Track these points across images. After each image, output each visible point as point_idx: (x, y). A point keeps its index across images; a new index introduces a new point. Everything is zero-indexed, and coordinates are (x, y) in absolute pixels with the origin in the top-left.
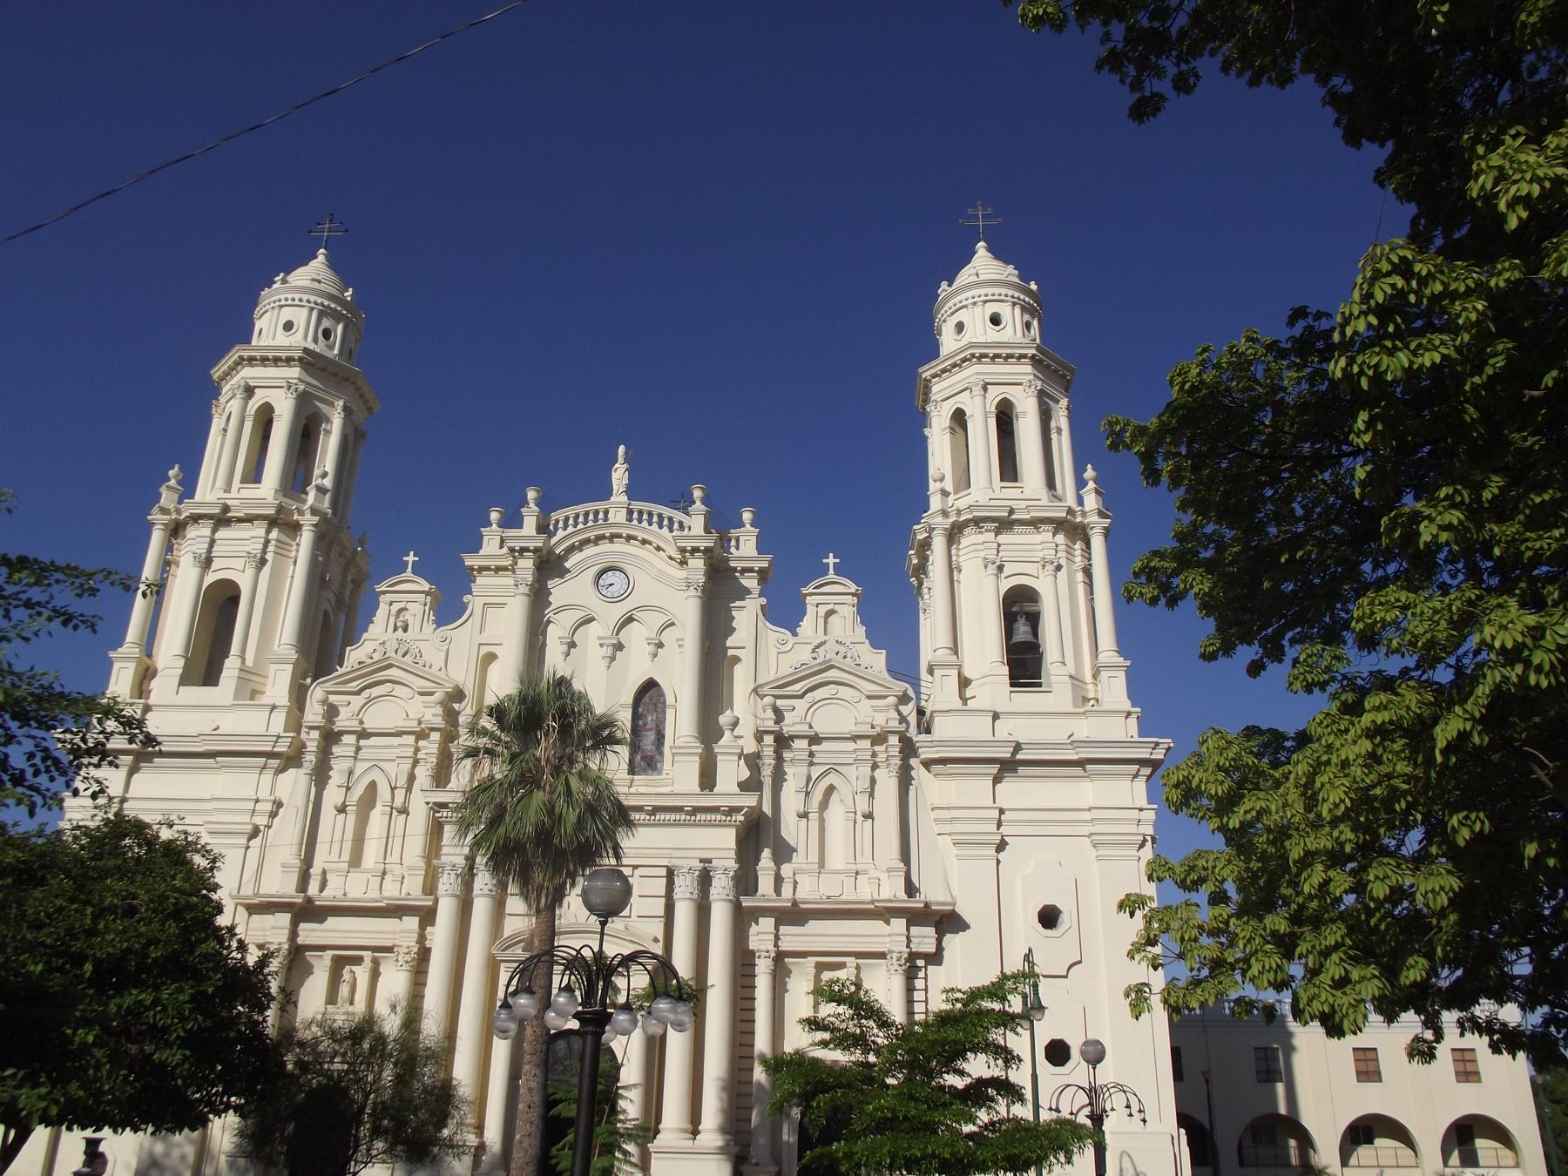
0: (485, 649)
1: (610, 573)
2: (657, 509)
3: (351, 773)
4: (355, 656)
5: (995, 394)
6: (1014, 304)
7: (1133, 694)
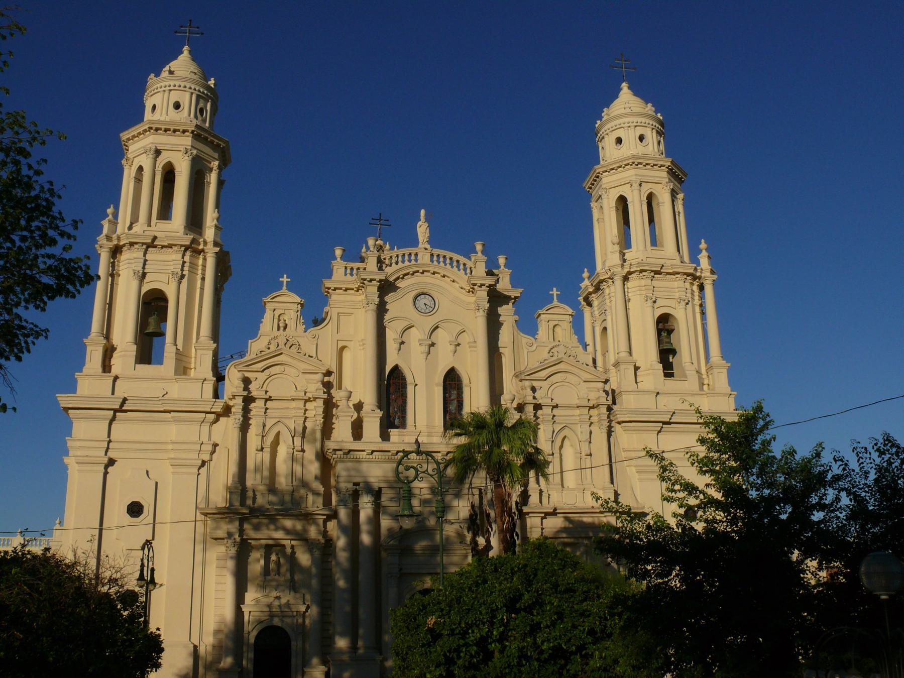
0: (341, 344)
1: (422, 296)
2: (449, 254)
3: (264, 426)
4: (256, 346)
5: (646, 189)
6: (653, 129)
7: (732, 382)
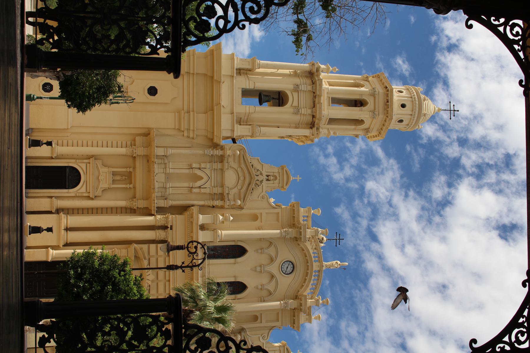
0: (259, 215)
